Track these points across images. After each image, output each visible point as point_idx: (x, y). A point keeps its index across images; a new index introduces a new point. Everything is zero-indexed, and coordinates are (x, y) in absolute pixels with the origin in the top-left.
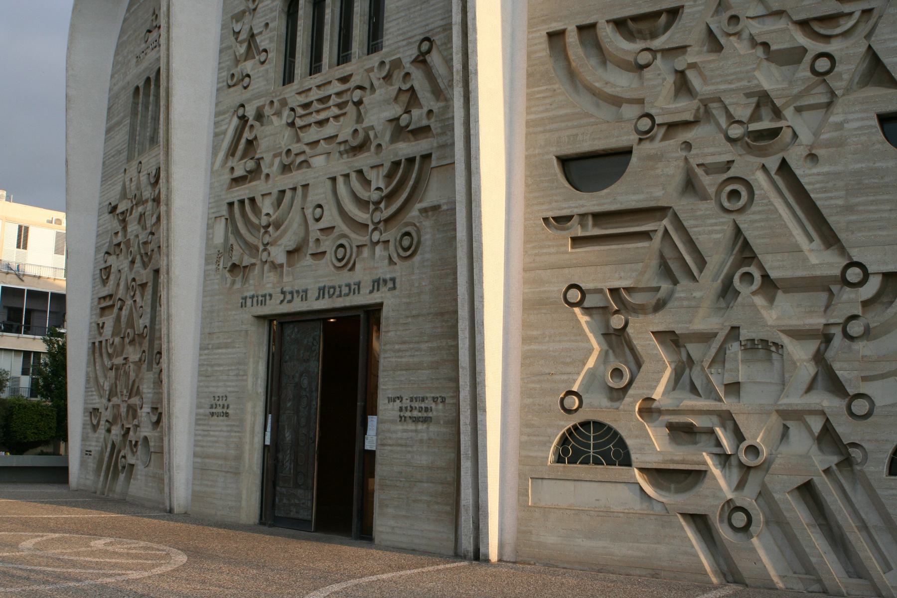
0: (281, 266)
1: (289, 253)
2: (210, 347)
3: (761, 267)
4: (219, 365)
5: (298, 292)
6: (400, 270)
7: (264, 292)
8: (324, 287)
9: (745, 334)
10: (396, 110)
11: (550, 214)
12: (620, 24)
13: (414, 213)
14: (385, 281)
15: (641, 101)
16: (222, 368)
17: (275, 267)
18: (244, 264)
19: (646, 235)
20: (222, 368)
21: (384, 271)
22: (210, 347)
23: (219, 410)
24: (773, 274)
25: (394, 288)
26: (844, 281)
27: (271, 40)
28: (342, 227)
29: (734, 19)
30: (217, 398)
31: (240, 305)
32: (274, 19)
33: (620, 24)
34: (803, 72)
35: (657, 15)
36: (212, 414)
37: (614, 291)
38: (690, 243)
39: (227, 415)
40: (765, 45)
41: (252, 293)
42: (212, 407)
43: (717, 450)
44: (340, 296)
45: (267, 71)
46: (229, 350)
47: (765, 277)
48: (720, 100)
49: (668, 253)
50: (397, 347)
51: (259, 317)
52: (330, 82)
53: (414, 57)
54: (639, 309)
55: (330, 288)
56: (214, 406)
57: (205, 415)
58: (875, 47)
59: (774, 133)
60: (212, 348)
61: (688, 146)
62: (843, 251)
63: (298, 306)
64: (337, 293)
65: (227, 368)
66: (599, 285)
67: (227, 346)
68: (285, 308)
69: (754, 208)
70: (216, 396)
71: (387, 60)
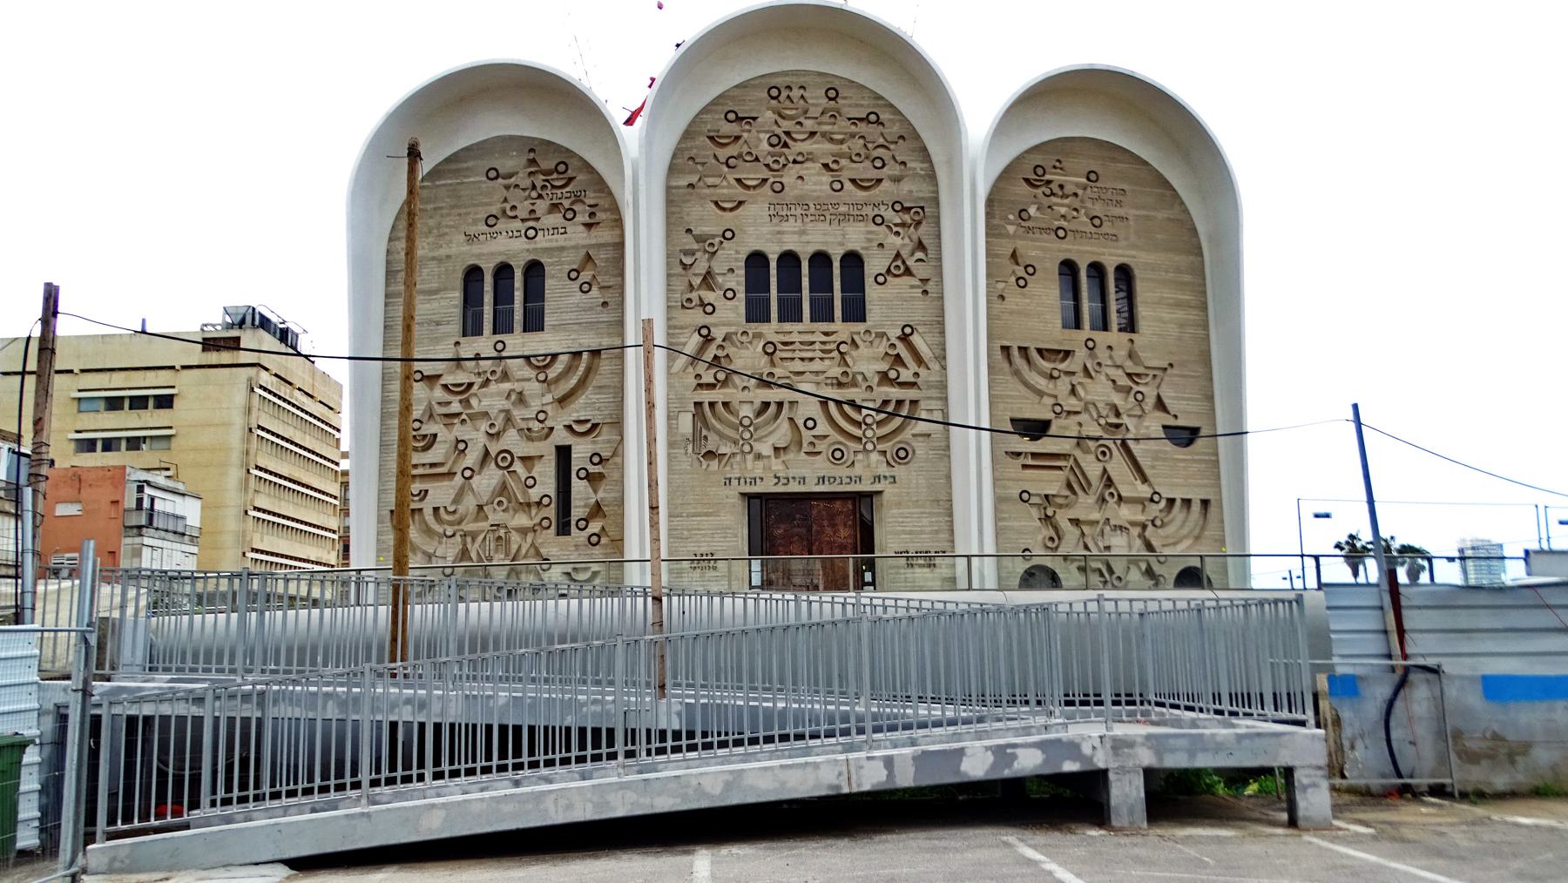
0: (769, 457)
1: (776, 449)
3: (1118, 491)
4: (699, 529)
5: (794, 478)
6: (899, 471)
7: (753, 476)
9: (1113, 522)
10: (884, 367)
11: (1009, 450)
12: (1040, 351)
13: (907, 434)
14: (885, 477)
15: (1056, 397)
17: (759, 456)
18: (720, 452)
19: (1060, 468)
21: (883, 470)
24: (1123, 494)
25: (895, 482)
26: (1152, 500)
27: (738, 283)
28: (835, 436)
29: (1099, 364)
32: (738, 268)
33: (1040, 351)
34: (1132, 399)
35: (1059, 352)
37: (1046, 496)
38: (1083, 474)
40: (1114, 381)
43: (1102, 579)
45: (737, 307)
47: (1119, 496)
48: (1094, 404)
49: (1072, 478)
50: (901, 520)
51: (743, 494)
52: (813, 332)
53: (898, 335)
54: (1061, 506)
55: (829, 478)
58: (1161, 394)
59: (1118, 426)
60: (687, 516)
61: (1080, 424)
62: (1150, 485)
63: (794, 487)
64: (838, 481)
66: (1039, 492)
67: (707, 515)
68: (780, 489)
69: (1114, 461)
71: (873, 331)
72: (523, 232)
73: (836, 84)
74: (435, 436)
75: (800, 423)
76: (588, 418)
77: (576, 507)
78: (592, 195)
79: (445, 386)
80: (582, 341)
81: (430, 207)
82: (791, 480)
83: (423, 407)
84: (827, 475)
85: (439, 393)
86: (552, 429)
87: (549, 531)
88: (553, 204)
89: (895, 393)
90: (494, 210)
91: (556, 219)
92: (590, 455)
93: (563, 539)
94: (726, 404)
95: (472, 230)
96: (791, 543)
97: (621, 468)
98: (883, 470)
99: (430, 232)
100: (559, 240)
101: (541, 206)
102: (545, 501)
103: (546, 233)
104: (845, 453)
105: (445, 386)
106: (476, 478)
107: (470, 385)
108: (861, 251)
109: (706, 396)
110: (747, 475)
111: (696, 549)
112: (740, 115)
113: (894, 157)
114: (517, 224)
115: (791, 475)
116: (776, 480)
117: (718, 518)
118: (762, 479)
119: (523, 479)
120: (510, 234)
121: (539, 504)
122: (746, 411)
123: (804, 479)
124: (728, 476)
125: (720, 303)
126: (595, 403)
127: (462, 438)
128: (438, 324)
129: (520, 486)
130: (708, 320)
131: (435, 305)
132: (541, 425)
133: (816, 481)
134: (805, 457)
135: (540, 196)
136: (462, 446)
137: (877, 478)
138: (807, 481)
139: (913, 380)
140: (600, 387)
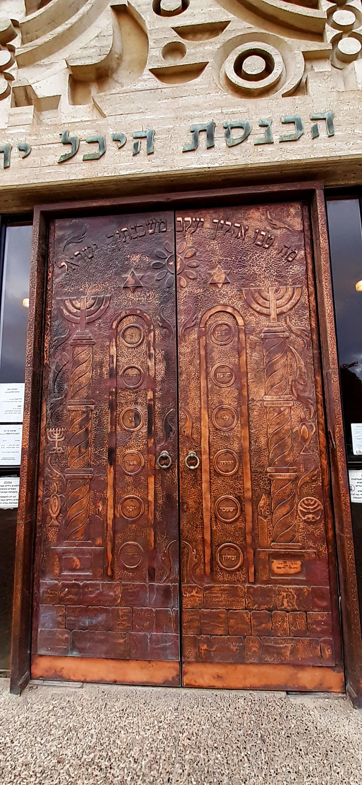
8: (213, 126)
55: (228, 129)
82: (111, 147)
84: (220, 122)
96: (115, 335)
104: (277, 60)
115: (111, 132)
116: (68, 150)
118: (25, 150)
123: (150, 138)
133: (189, 140)
134: (155, 82)
138: (157, 145)
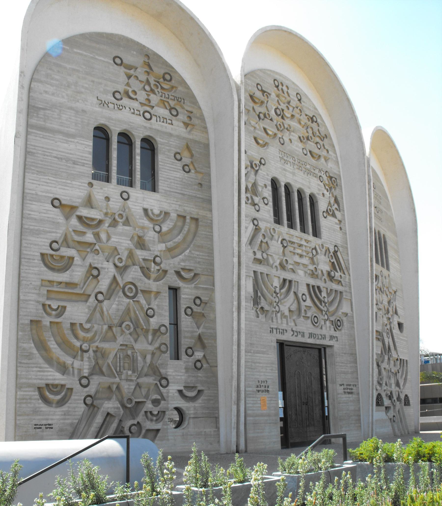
2: (252, 351)
4: (260, 363)
6: (337, 334)
16: (261, 365)
20: (261, 365)
22: (252, 351)
23: (263, 389)
25: (337, 341)
30: (260, 382)
31: (269, 331)
36: (259, 391)
39: (268, 391)
41: (276, 327)
42: (257, 387)
44: (318, 339)
46: (265, 355)
56: (259, 386)
57: (253, 392)
60: (254, 353)
63: (299, 339)
64: (317, 337)
65: (265, 365)
67: (263, 353)
68: (294, 339)
70: (260, 380)
72: (141, 113)
73: (300, 92)
74: (72, 259)
75: (300, 295)
76: (192, 268)
77: (185, 337)
78: (189, 104)
79: (80, 218)
80: (186, 208)
81: (68, 66)
82: (299, 333)
83: (61, 232)
85: (74, 221)
86: (165, 272)
87: (166, 355)
88: (161, 100)
89: (335, 286)
90: (121, 88)
91: (163, 112)
92: (193, 297)
93: (176, 362)
94: (267, 275)
95: (103, 97)
97: (213, 310)
98: (332, 333)
99: (68, 86)
100: (168, 128)
101: (155, 99)
102: (163, 329)
103: (158, 119)
105: (80, 218)
106: (106, 303)
107: (100, 222)
108: (317, 195)
109: (260, 268)
110: (280, 328)
111: (258, 377)
112: (263, 89)
113: (323, 145)
114: (135, 105)
117: (268, 356)
119: (146, 310)
120: (132, 110)
121: (156, 332)
122: (276, 283)
124: (272, 326)
125: (262, 205)
126: (196, 258)
127: (96, 265)
128: (75, 163)
129: (143, 315)
130: (257, 215)
131: (72, 146)
132: (158, 268)
135: (152, 91)
136: (95, 272)
137: (332, 337)
139: (339, 279)
140: (199, 246)
